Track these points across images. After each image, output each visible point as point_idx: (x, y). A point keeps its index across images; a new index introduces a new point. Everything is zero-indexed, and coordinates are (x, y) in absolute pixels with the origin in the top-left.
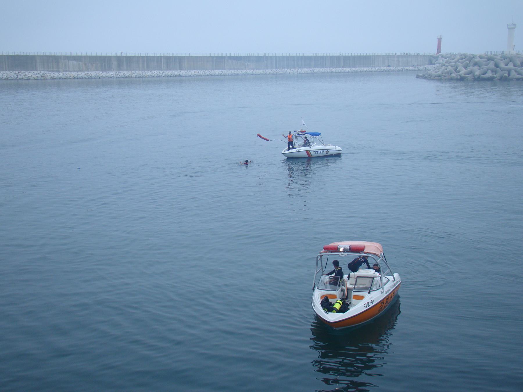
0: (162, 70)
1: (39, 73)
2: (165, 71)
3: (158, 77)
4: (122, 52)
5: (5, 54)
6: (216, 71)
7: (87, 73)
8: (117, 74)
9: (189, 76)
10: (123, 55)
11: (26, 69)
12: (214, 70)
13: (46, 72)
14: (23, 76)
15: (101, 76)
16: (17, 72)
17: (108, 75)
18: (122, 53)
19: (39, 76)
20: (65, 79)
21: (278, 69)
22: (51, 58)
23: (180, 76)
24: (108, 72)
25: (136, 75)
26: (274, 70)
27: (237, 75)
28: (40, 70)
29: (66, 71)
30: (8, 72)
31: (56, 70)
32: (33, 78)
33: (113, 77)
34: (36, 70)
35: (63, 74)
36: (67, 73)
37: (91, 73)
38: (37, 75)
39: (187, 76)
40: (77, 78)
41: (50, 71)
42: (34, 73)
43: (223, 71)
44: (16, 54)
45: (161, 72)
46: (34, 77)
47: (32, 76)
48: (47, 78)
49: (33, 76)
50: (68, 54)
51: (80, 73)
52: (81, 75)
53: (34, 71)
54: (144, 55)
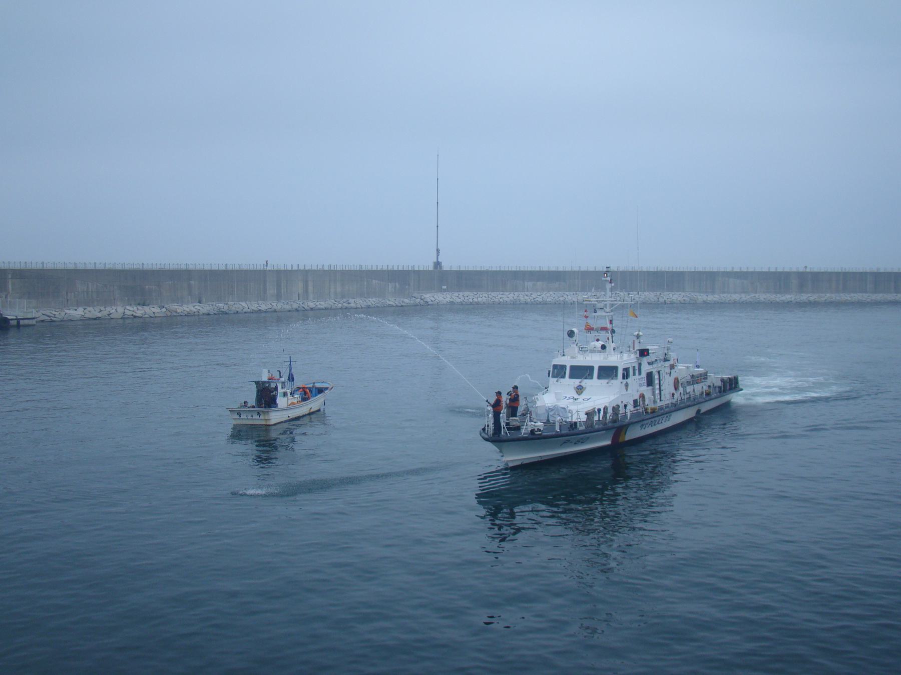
0: (867, 293)
2: (871, 295)
5: (644, 270)
8: (797, 297)
10: (808, 270)
11: (670, 289)
13: (697, 294)
14: (666, 299)
15: (773, 301)
16: (658, 293)
17: (783, 298)
18: (806, 267)
20: (722, 303)
25: (826, 300)
29: (724, 292)
30: (646, 293)
32: (679, 302)
33: (791, 301)
34: (684, 291)
35: (720, 296)
36: (725, 295)
37: (759, 296)
38: (684, 298)
44: (659, 269)
46: (680, 301)
48: (698, 302)
49: (678, 299)
50: (729, 270)
51: (743, 295)
52: (746, 299)
54: (840, 271)
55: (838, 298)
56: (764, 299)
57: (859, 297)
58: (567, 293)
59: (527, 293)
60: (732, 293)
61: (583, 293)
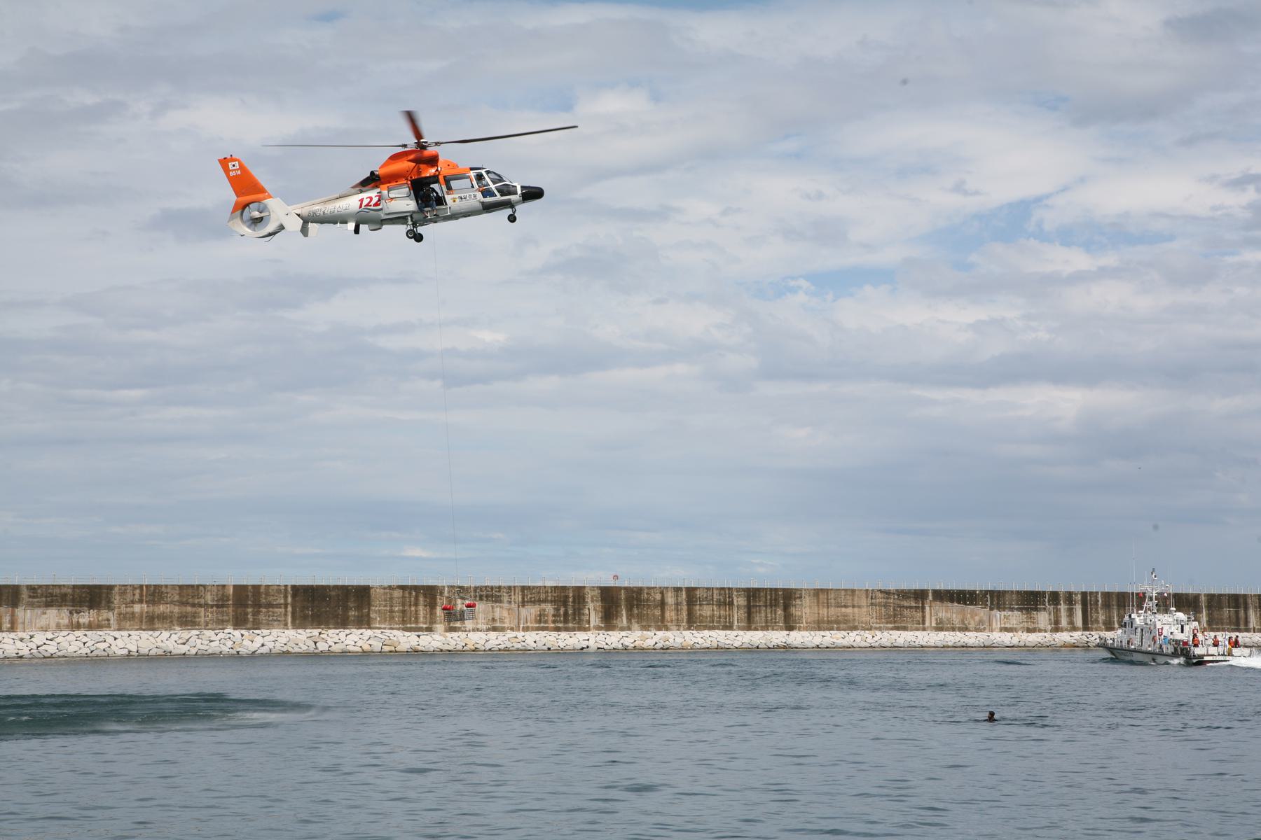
2: (741, 633)
3: (722, 648)
6: (896, 633)
7: (515, 636)
8: (599, 638)
11: (343, 623)
12: (891, 632)
16: (316, 632)
19: (377, 646)
21: (1092, 633)
22: (414, 594)
23: (787, 648)
24: (575, 634)
25: (656, 643)
26: (1079, 633)
27: (963, 647)
28: (380, 628)
31: (425, 626)
33: (588, 647)
34: (369, 626)
35: (446, 637)
38: (370, 642)
40: (483, 648)
41: (410, 630)
42: (361, 634)
47: (355, 642)
51: (493, 635)
53: (364, 630)
55: (679, 640)
56: (535, 642)
58: (117, 634)
59: (21, 635)
60: (469, 631)
61: (151, 633)
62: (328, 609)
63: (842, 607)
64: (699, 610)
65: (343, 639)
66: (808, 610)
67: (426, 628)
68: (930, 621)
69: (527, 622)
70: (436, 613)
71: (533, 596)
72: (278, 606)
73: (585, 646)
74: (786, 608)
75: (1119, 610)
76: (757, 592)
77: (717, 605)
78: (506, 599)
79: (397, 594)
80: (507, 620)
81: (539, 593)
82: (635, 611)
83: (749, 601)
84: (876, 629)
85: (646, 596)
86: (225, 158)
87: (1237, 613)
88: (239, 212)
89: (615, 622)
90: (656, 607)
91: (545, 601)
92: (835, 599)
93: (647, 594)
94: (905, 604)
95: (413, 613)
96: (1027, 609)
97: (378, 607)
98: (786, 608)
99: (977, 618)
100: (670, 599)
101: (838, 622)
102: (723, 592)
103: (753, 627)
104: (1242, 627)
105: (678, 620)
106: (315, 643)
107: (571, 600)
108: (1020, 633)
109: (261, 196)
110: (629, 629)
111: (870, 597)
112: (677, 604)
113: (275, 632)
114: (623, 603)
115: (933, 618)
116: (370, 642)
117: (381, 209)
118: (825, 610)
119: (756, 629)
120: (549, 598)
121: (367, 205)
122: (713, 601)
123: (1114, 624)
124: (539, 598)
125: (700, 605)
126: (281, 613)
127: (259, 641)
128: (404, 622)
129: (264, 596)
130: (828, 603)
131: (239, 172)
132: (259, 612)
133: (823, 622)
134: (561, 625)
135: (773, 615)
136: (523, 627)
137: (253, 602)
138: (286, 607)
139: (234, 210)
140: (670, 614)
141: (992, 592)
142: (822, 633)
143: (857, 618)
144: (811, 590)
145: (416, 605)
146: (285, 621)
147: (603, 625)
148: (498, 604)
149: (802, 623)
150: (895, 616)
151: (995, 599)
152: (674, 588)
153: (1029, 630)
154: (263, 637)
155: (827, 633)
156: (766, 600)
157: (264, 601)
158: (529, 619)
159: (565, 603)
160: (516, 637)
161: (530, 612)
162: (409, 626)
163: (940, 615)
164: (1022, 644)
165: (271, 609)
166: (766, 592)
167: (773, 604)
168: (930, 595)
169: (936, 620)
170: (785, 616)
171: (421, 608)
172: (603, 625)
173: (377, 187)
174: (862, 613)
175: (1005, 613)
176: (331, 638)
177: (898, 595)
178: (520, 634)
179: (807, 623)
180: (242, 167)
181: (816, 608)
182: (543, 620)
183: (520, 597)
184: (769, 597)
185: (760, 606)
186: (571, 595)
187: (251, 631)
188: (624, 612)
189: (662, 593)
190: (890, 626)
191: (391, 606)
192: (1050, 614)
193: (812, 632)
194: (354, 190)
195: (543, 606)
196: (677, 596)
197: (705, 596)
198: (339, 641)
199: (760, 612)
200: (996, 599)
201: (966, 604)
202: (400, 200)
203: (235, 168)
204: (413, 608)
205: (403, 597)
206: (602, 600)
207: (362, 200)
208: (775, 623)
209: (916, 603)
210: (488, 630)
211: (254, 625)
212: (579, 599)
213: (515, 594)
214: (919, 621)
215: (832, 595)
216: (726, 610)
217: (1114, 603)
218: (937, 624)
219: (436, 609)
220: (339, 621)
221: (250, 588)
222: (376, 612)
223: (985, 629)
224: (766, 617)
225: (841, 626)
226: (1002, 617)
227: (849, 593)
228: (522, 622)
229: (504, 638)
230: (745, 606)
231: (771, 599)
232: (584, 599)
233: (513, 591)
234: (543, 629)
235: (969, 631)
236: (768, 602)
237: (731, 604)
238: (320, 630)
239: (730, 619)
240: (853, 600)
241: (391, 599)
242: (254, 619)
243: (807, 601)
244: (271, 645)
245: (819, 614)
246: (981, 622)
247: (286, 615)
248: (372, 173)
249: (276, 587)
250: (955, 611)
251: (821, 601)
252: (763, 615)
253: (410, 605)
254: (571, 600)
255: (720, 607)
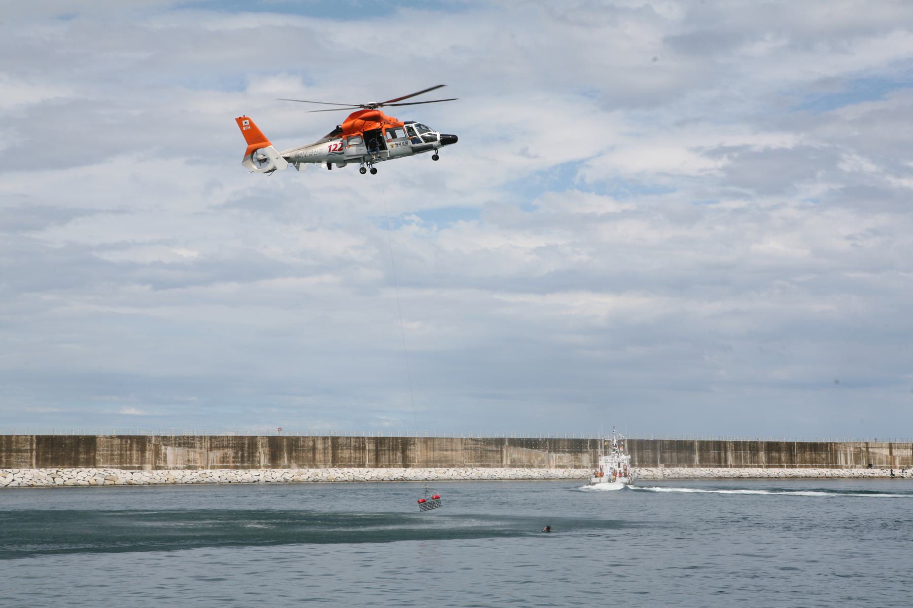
1: (99, 473)
2: (371, 469)
3: (357, 481)
4: (281, 429)
6: (482, 470)
7: (204, 472)
8: (267, 474)
9: (423, 480)
12: (478, 468)
16: (54, 470)
19: (101, 480)
22: (129, 442)
23: (403, 480)
24: (249, 471)
25: (309, 477)
27: (529, 479)
28: (103, 467)
31: (137, 465)
33: (258, 480)
34: (95, 467)
35: (152, 473)
39: (419, 480)
40: (181, 482)
42: (89, 472)
43: (497, 469)
45: (364, 470)
46: (88, 481)
47: (84, 478)
51: (188, 472)
55: (326, 475)
56: (219, 477)
57: (354, 474)
60: (171, 469)
62: (64, 453)
63: (443, 450)
64: (341, 453)
65: (75, 476)
66: (419, 453)
67: (138, 467)
68: (506, 461)
69: (213, 463)
70: (145, 456)
71: (218, 443)
72: (26, 451)
73: (257, 480)
74: (404, 451)
75: (638, 452)
76: (383, 440)
77: (353, 449)
78: (198, 445)
79: (117, 442)
80: (199, 461)
81: (223, 441)
82: (294, 454)
83: (377, 447)
84: (468, 466)
85: (302, 443)
86: (240, 118)
87: (719, 454)
88: (249, 156)
89: (279, 462)
90: (309, 451)
91: (227, 447)
92: (439, 445)
93: (303, 441)
94: (489, 448)
95: (128, 456)
96: (574, 452)
97: (101, 452)
98: (404, 451)
99: (539, 459)
100: (320, 446)
101: (440, 461)
102: (358, 440)
103: (379, 466)
104: (723, 464)
105: (325, 460)
106: (54, 478)
107: (246, 446)
108: (569, 469)
109: (264, 143)
110: (289, 467)
111: (464, 443)
112: (325, 449)
113: (23, 470)
114: (285, 448)
115: (509, 459)
116: (95, 478)
117: (343, 153)
118: (432, 453)
119: (382, 467)
120: (230, 445)
121: (334, 150)
122: (351, 445)
123: (635, 462)
124: (223, 445)
125: (342, 449)
126: (27, 456)
127: (10, 477)
128: (121, 463)
129: (14, 444)
130: (434, 448)
131: (249, 127)
132: (10, 456)
133: (430, 461)
134: (239, 464)
135: (394, 457)
136: (211, 466)
137: (6, 448)
138: (31, 452)
139: (247, 154)
140: (319, 456)
141: (550, 440)
142: (429, 469)
143: (454, 458)
144: (422, 438)
145: (131, 450)
146: (30, 462)
147: (270, 464)
148: (192, 449)
149: (415, 462)
150: (481, 457)
151: (553, 445)
152: (323, 437)
153: (576, 467)
154: (14, 474)
155: (433, 469)
156: (389, 446)
157: (15, 447)
158: (215, 460)
159: (242, 449)
160: (205, 474)
161: (216, 455)
162: (125, 465)
163: (513, 456)
164: (571, 477)
165: (20, 454)
166: (389, 440)
167: (394, 449)
168: (507, 442)
169: (511, 460)
170: (403, 457)
171: (134, 452)
172: (270, 464)
173: (341, 137)
174: (458, 455)
175: (559, 455)
176: (66, 475)
177: (484, 442)
178: (208, 471)
179: (418, 462)
180: (251, 124)
181: (425, 451)
182: (225, 461)
183: (209, 444)
184: (391, 444)
185: (384, 450)
186: (246, 442)
187: (4, 470)
188: (286, 455)
189: (314, 441)
190: (478, 464)
191: (112, 451)
192: (590, 455)
193: (422, 469)
194: (326, 139)
195: (226, 450)
196: (325, 443)
197: (345, 443)
198: (71, 477)
199: (385, 454)
200: (553, 445)
201: (531, 448)
202: (355, 147)
203: (247, 124)
204: (128, 453)
205: (121, 444)
206: (269, 446)
207: (330, 147)
208: (396, 462)
209: (496, 448)
210: (185, 468)
211: (6, 465)
212: (252, 446)
213: (205, 442)
214: (498, 461)
215: (437, 442)
216: (360, 454)
217: (635, 447)
218: (511, 462)
219: (145, 453)
220: (72, 462)
221: (4, 437)
222: (100, 455)
223: (545, 466)
224: (389, 458)
225: (444, 464)
226: (557, 458)
227: (449, 440)
228: (210, 462)
229: (196, 474)
230: (374, 450)
231: (393, 445)
232: (256, 445)
233: (203, 440)
234: (226, 467)
235: (534, 467)
236: (391, 447)
237: (364, 449)
238: (57, 469)
239: (363, 460)
240: (452, 446)
241: (112, 445)
242: (7, 461)
243: (419, 446)
244: (19, 480)
245: (427, 455)
246: (542, 461)
247: (31, 458)
248: (337, 127)
249: (24, 437)
250: (524, 453)
251: (428, 447)
252: (387, 456)
253: (126, 450)
254: (246, 446)
255: (356, 451)
